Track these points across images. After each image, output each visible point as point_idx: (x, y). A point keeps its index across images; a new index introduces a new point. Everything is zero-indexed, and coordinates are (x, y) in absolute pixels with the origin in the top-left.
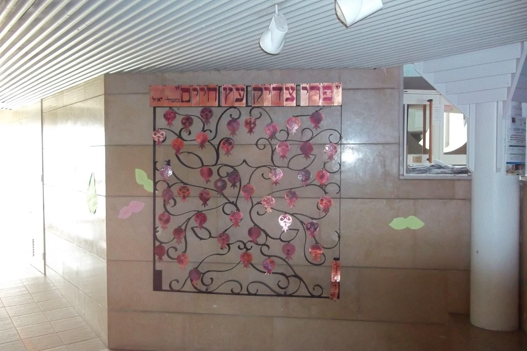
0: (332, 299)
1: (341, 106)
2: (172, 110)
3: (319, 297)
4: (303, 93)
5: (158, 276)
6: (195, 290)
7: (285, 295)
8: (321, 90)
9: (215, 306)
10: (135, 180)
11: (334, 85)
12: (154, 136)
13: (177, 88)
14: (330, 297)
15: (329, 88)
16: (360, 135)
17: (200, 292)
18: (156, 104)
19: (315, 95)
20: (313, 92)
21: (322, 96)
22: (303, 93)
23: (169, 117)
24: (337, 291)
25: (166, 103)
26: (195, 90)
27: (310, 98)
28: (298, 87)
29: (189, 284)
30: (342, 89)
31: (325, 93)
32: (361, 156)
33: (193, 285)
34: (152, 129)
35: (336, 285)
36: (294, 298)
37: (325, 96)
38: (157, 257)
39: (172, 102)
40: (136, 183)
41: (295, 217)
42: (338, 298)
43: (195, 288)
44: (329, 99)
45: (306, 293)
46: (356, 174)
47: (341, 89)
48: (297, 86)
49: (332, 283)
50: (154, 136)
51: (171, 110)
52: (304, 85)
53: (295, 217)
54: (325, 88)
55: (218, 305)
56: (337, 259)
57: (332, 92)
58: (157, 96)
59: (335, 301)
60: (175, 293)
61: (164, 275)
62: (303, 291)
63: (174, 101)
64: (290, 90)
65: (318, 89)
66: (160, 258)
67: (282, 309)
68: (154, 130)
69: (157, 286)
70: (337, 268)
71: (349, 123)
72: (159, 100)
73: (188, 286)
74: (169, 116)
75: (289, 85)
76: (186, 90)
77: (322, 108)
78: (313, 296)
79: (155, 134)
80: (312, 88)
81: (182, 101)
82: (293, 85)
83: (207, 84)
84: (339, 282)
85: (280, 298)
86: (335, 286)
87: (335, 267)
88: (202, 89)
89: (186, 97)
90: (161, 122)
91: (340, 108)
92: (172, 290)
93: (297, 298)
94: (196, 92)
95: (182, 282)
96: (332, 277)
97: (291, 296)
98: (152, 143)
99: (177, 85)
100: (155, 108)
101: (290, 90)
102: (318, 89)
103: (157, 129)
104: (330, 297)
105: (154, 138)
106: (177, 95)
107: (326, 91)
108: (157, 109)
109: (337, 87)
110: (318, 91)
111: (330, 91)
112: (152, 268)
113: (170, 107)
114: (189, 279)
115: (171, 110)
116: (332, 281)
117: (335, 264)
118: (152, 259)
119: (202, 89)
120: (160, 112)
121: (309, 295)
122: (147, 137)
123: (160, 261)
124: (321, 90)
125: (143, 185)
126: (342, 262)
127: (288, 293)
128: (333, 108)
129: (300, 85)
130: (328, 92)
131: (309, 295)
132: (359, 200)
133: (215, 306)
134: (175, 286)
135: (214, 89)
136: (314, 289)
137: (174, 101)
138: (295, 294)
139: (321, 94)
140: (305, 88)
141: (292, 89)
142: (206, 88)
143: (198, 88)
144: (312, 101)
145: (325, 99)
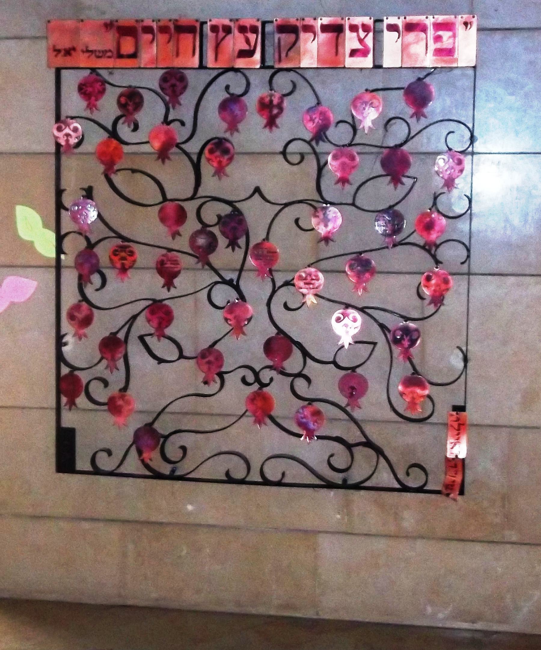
0: (448, 495)
1: (474, 67)
2: (98, 75)
3: (420, 490)
4: (389, 37)
5: (65, 440)
6: (148, 473)
7: (345, 486)
8: (431, 32)
9: (190, 507)
10: (15, 229)
11: (459, 20)
12: (56, 133)
13: (109, 26)
14: (444, 491)
15: (447, 26)
16: (517, 133)
17: (158, 476)
18: (60, 61)
19: (417, 42)
20: (411, 37)
21: (432, 46)
22: (389, 37)
23: (91, 90)
24: (458, 479)
25: (82, 60)
26: (148, 30)
27: (404, 48)
28: (377, 24)
29: (133, 458)
30: (479, 30)
31: (438, 39)
32: (517, 179)
33: (143, 461)
34: (53, 120)
35: (457, 465)
36: (362, 492)
37: (439, 45)
38: (64, 400)
39: (98, 57)
40: (16, 237)
41: (462, 373)
42: (462, 493)
43: (147, 466)
44: (447, 52)
45: (391, 482)
46: (507, 220)
47: (474, 29)
48: (376, 21)
49: (447, 460)
50: (56, 133)
51: (94, 75)
52: (392, 20)
53: (462, 373)
54: (438, 26)
55: (196, 504)
56: (460, 409)
57: (454, 36)
58: (65, 43)
59: (455, 500)
60: (103, 480)
61: (79, 440)
62: (384, 477)
63: (101, 54)
64: (360, 30)
65: (423, 29)
66: (72, 403)
67: (339, 516)
68: (58, 119)
69: (65, 461)
70: (459, 427)
71: (491, 105)
72: (68, 52)
73: (133, 464)
74: (90, 89)
75: (358, 20)
76: (127, 31)
77: (430, 72)
78: (405, 489)
79: (59, 129)
80: (410, 27)
81: (120, 56)
82: (368, 21)
83: (174, 16)
84: (463, 460)
85: (332, 493)
86: (455, 466)
87: (456, 425)
88: (164, 29)
89: (128, 46)
90: (73, 103)
91: (471, 72)
92: (97, 471)
93: (373, 492)
94: (149, 37)
95: (118, 454)
96: (449, 446)
97: (357, 487)
98: (53, 149)
99: (108, 17)
100: (58, 72)
101: (360, 30)
102: (423, 29)
103: (63, 118)
104: (444, 491)
105: (56, 138)
106: (108, 41)
107: (440, 33)
108: (64, 73)
109: (466, 24)
110: (423, 35)
111: (450, 34)
112: (53, 424)
113: (93, 70)
114: (134, 448)
115: (94, 75)
116: (449, 456)
117: (454, 418)
118: (53, 404)
119: (164, 29)
120: (71, 80)
121: (397, 486)
122: (41, 135)
123: (70, 409)
124: (431, 32)
125: (32, 243)
126: (472, 415)
127: (350, 482)
128: (456, 72)
129: (382, 21)
130: (446, 35)
131: (397, 486)
132: (512, 279)
133: (190, 507)
134: (105, 463)
135: (190, 29)
136: (408, 474)
137: (101, 54)
138: (367, 484)
139: (431, 42)
140: (393, 28)
141: (366, 29)
142: (172, 27)
143: (155, 25)
144: (410, 56)
145: (439, 52)
